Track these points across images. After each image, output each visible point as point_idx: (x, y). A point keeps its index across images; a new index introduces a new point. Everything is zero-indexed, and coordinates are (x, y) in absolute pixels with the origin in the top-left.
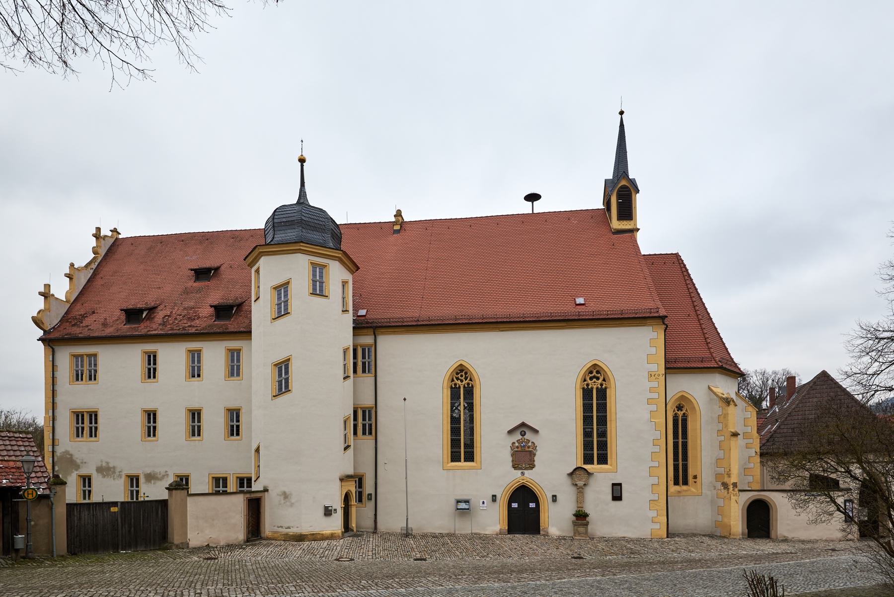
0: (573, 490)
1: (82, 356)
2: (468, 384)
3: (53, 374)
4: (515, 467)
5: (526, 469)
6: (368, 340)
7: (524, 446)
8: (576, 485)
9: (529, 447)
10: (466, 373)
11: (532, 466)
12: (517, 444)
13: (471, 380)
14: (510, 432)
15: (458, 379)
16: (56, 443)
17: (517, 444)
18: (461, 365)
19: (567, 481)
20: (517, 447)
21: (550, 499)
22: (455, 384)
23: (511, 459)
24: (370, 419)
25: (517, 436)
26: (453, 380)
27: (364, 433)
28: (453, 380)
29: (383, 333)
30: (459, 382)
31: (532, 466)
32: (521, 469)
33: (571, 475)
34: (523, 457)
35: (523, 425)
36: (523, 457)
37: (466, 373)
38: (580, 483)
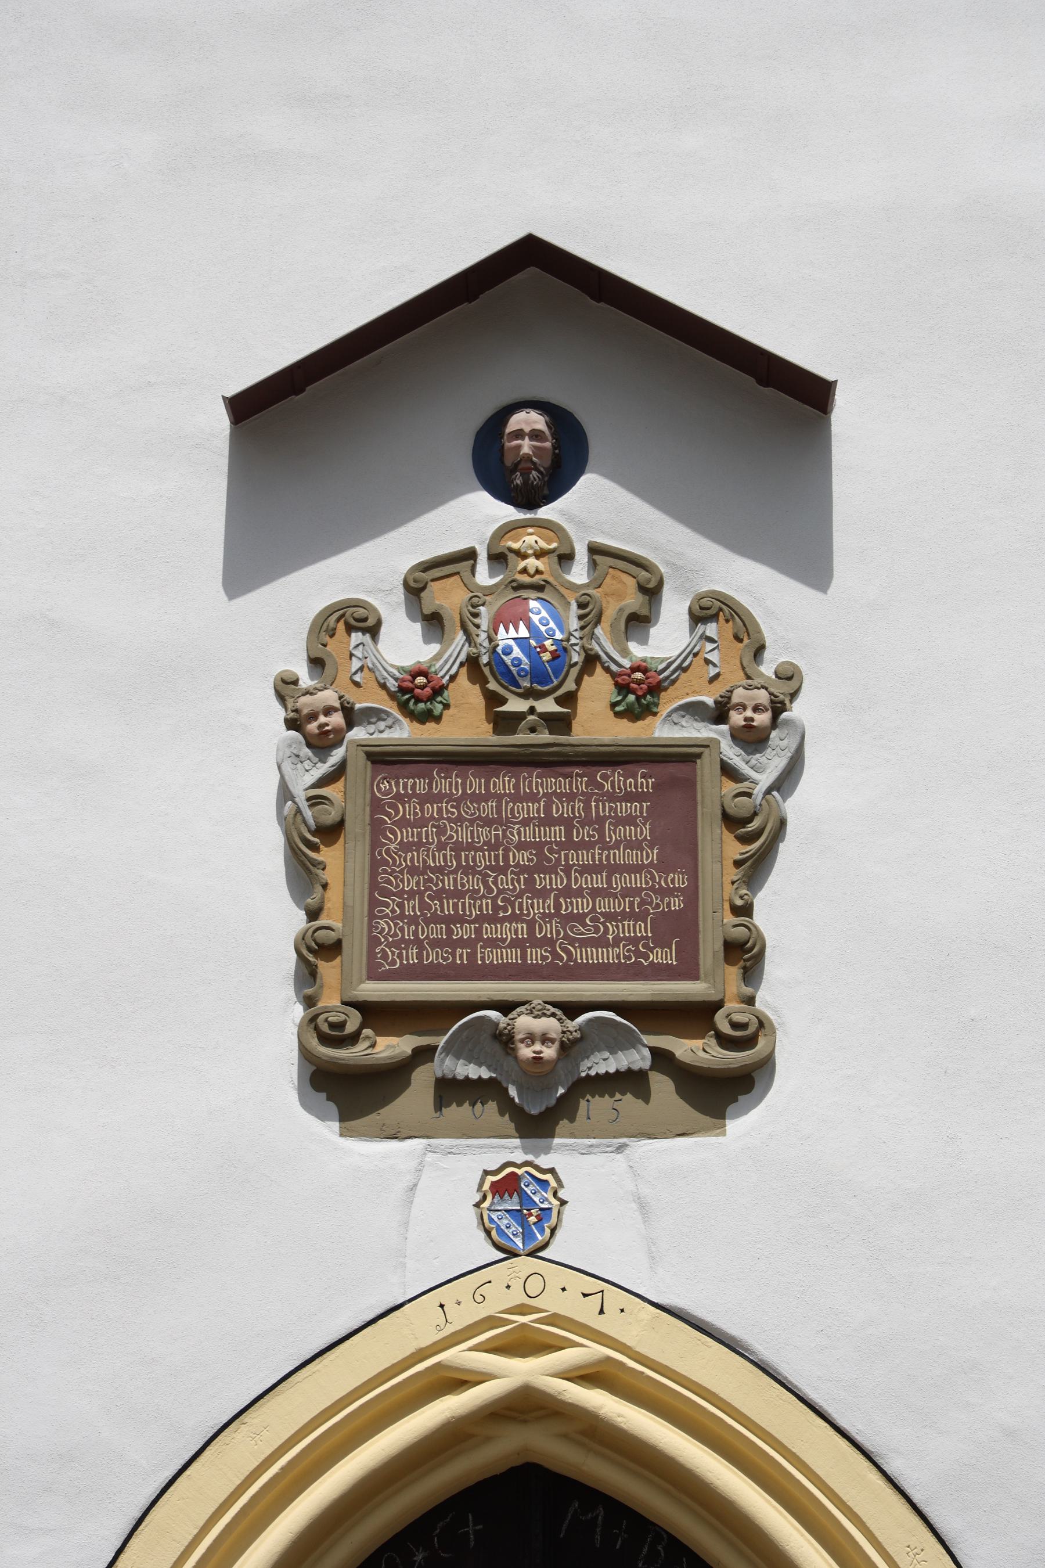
4: (347, 1088)
7: (548, 672)
9: (639, 693)
20: (418, 695)
23: (281, 922)
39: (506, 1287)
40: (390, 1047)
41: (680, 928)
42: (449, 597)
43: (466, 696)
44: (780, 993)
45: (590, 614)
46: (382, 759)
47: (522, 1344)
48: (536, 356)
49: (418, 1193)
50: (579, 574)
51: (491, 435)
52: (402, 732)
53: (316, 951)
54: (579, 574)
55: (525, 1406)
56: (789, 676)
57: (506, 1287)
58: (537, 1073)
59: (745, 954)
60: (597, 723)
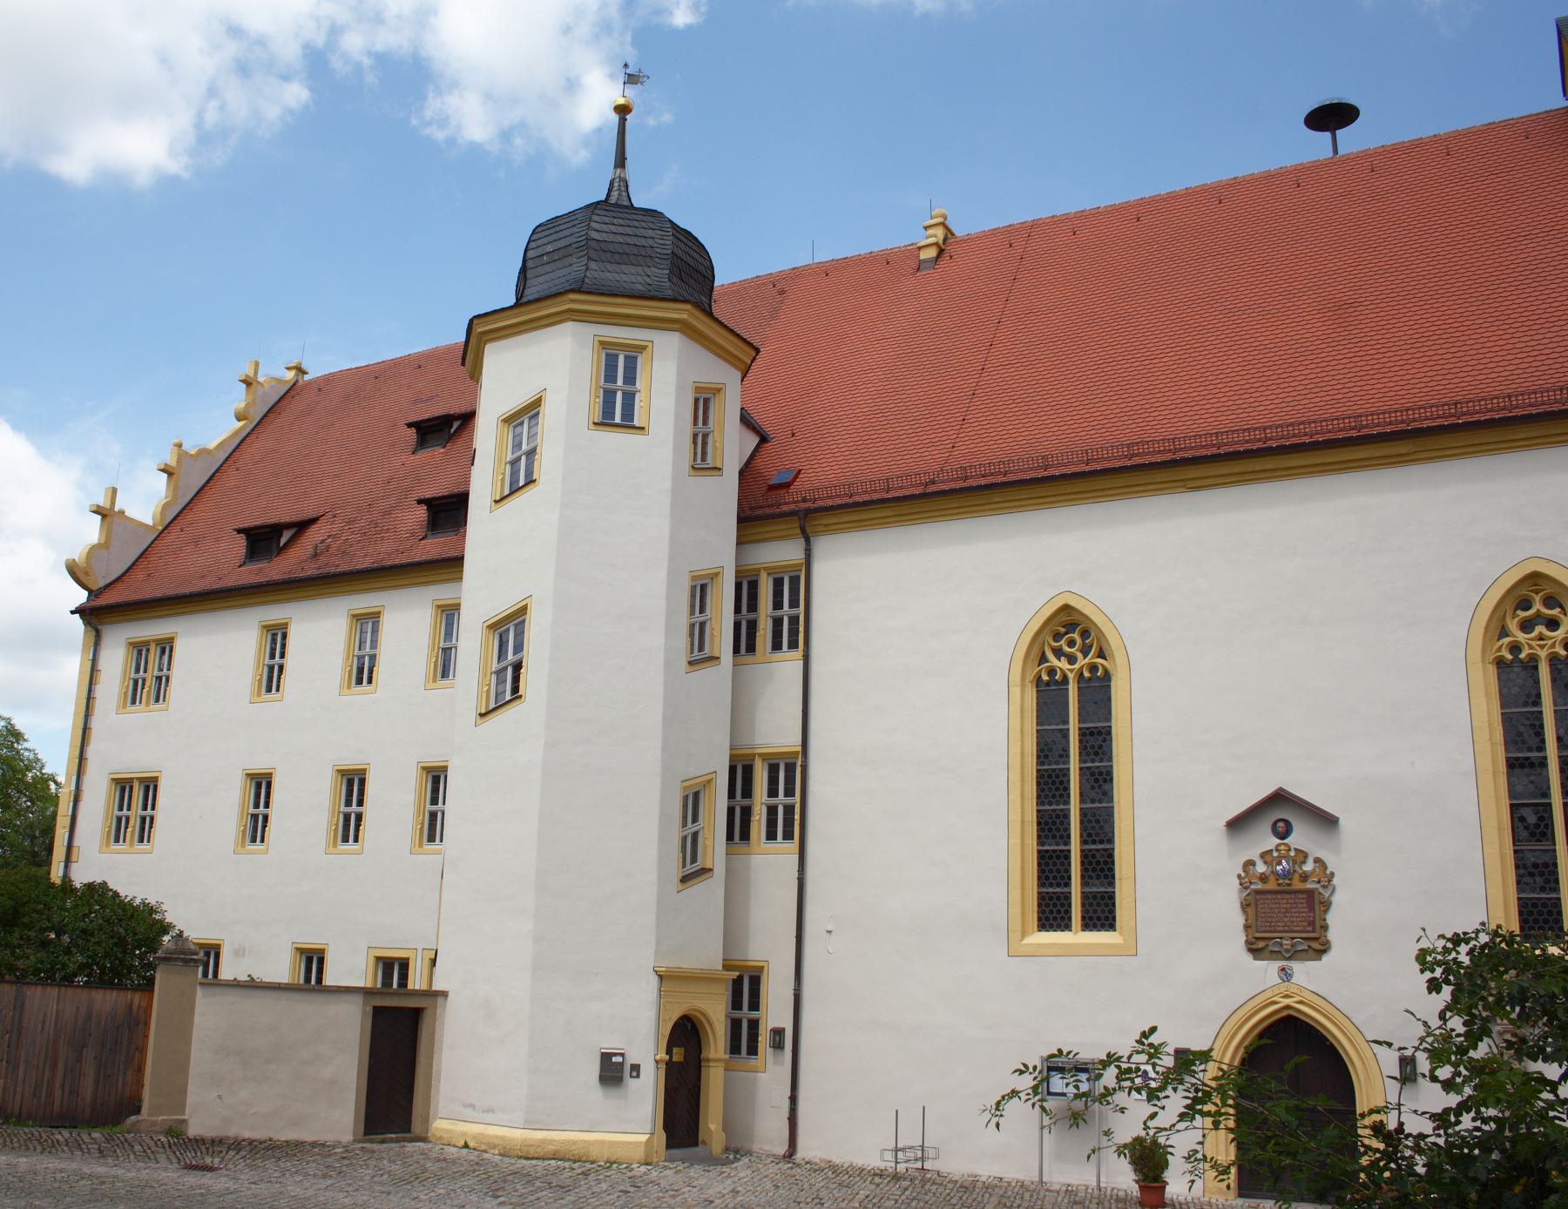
1: (146, 644)
2: (1093, 668)
3: (90, 690)
5: (1294, 955)
6: (782, 552)
7: (1287, 875)
9: (1305, 877)
10: (1085, 634)
11: (1317, 947)
12: (1261, 868)
13: (1101, 655)
14: (1238, 824)
15: (1058, 653)
16: (74, 858)
17: (1261, 868)
18: (1066, 608)
20: (1263, 878)
22: (1052, 672)
23: (1239, 919)
24: (789, 792)
26: (1043, 659)
27: (771, 836)
29: (830, 530)
30: (1063, 664)
31: (1317, 947)
32: (1275, 955)
34: (1287, 913)
36: (1287, 913)
37: (1085, 634)
39: (1284, 987)
40: (1261, 944)
41: (1312, 923)
42: (1268, 858)
43: (1272, 878)
44: (1332, 935)
45: (1295, 862)
46: (1257, 892)
47: (1287, 996)
49: (1268, 970)
50: (1292, 854)
51: (1274, 825)
52: (1259, 886)
53: (1247, 927)
54: (1292, 854)
55: (1288, 1007)
56: (1332, 874)
57: (1284, 987)
58: (1287, 951)
59: (1325, 928)
60: (1297, 885)
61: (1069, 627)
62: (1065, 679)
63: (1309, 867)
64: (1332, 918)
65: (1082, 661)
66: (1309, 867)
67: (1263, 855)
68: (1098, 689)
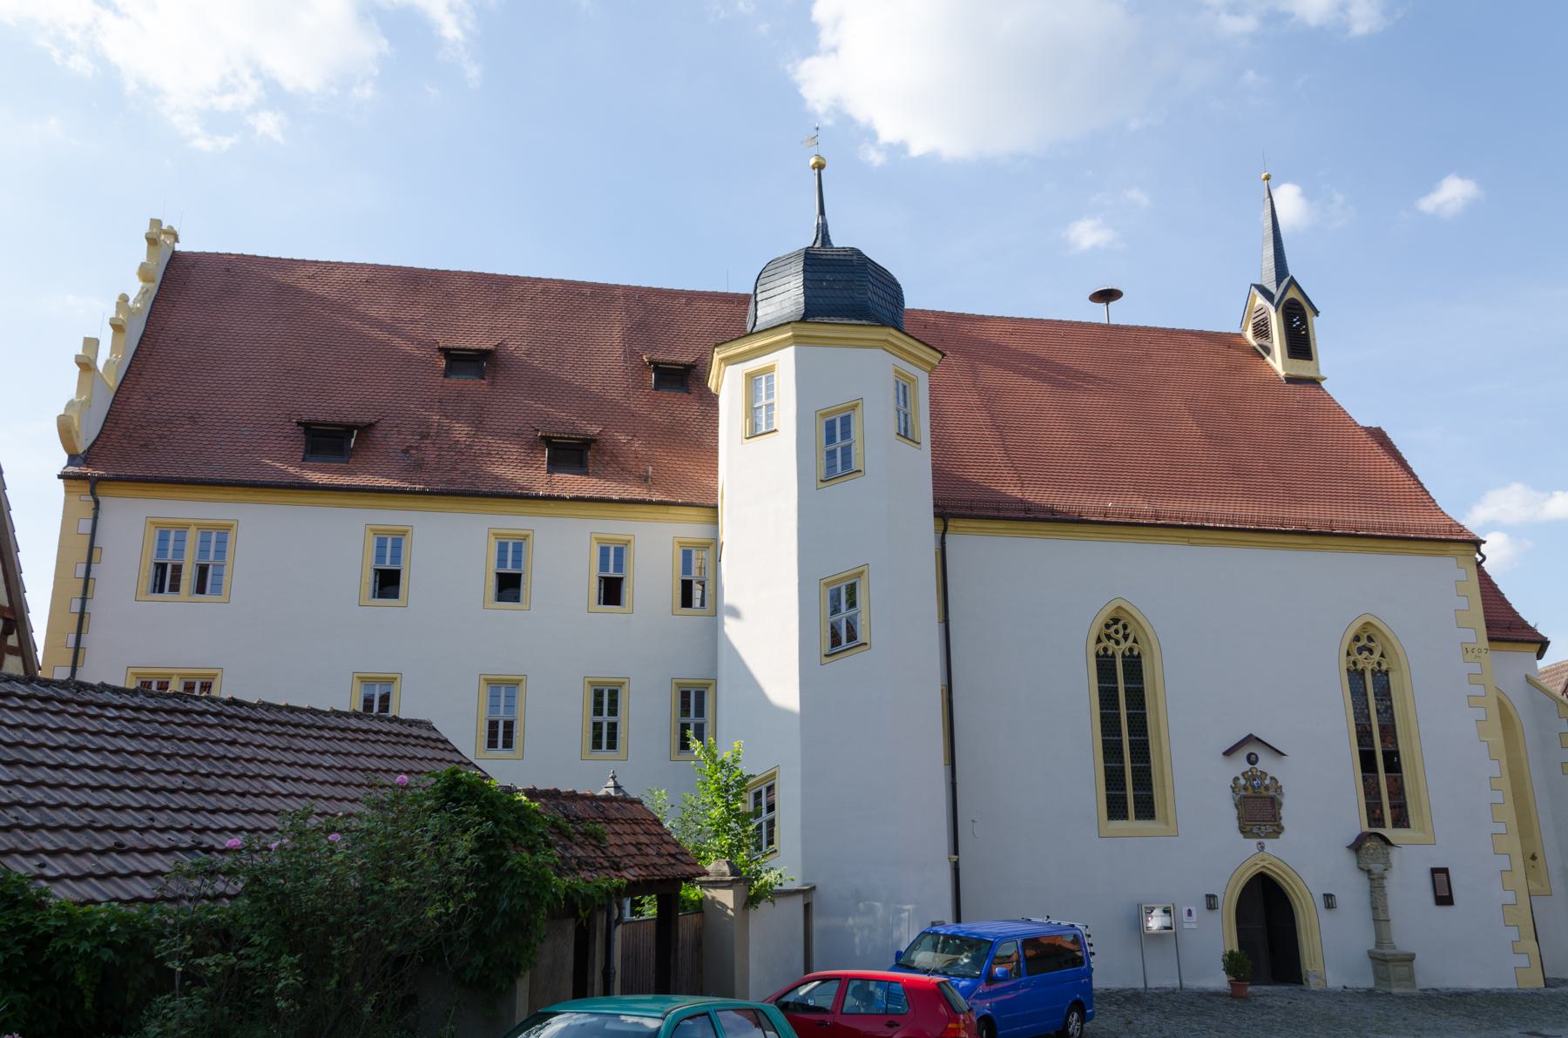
0: (1363, 880)
2: (1131, 650)
8: (1369, 872)
9: (1267, 788)
10: (1125, 627)
11: (1277, 831)
13: (1135, 641)
14: (1228, 753)
15: (1109, 637)
19: (1348, 859)
21: (1321, 903)
25: (1240, 765)
28: (1099, 640)
33: (1357, 846)
35: (1250, 739)
37: (1125, 627)
38: (1377, 868)
44: (1284, 823)
48: (1249, 745)
60: (1265, 793)
61: (1117, 624)
62: (1113, 656)
63: (1267, 782)
64: (1284, 812)
65: (1124, 646)
66: (1267, 782)
67: (1243, 774)
68: (1134, 665)
